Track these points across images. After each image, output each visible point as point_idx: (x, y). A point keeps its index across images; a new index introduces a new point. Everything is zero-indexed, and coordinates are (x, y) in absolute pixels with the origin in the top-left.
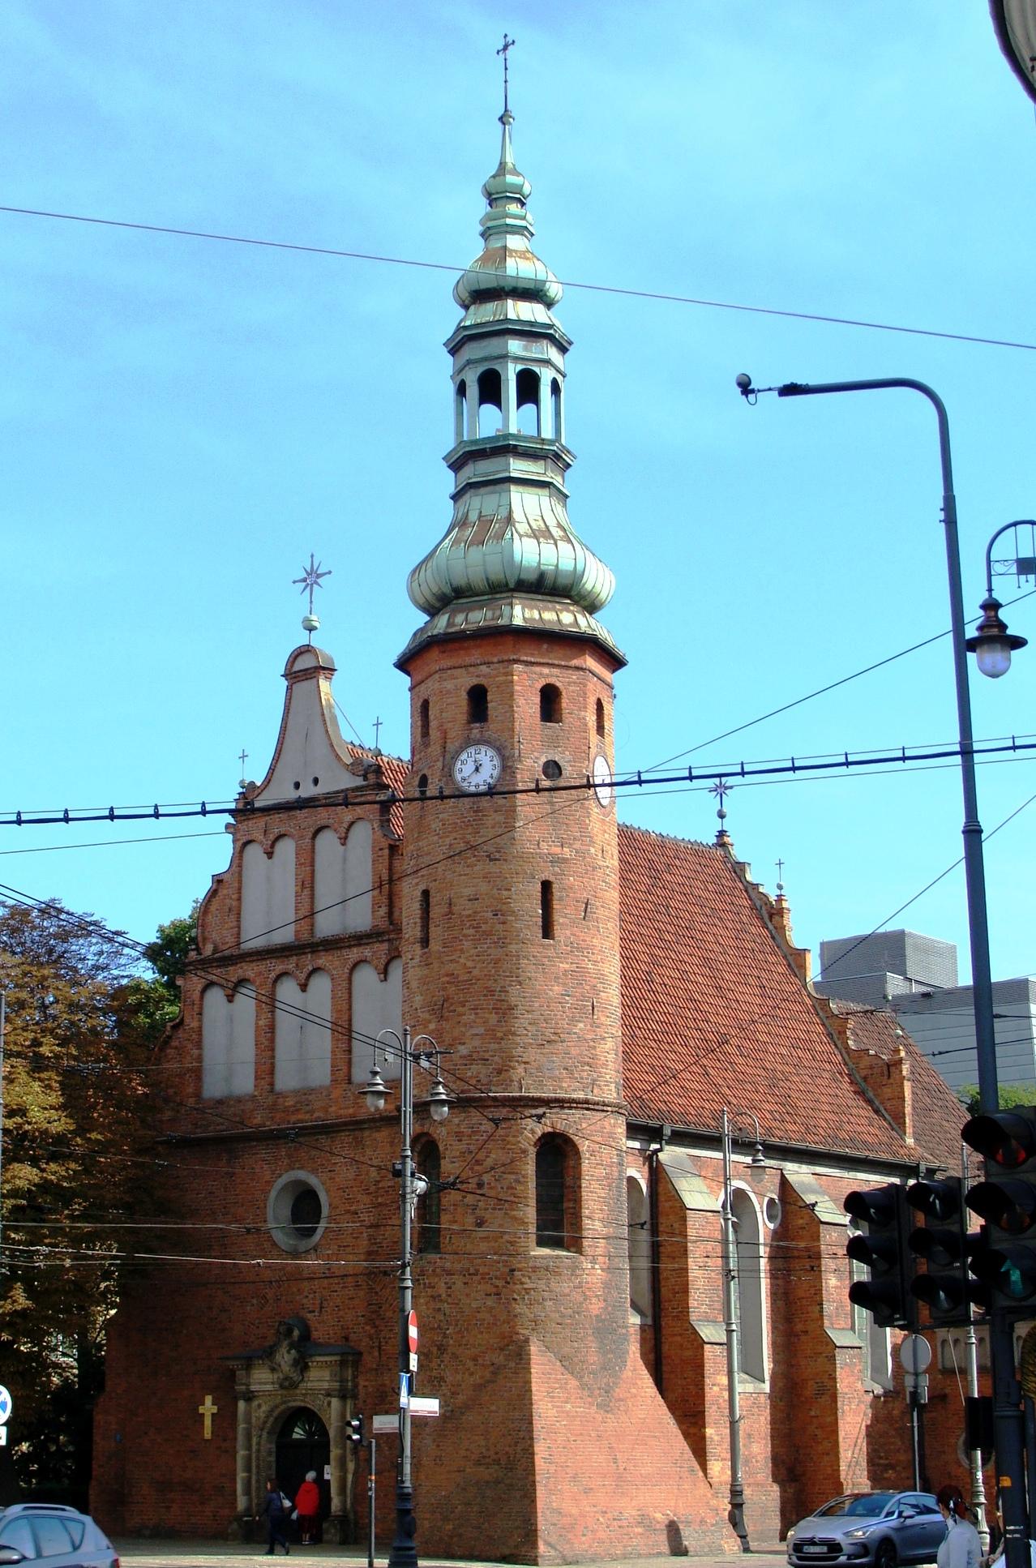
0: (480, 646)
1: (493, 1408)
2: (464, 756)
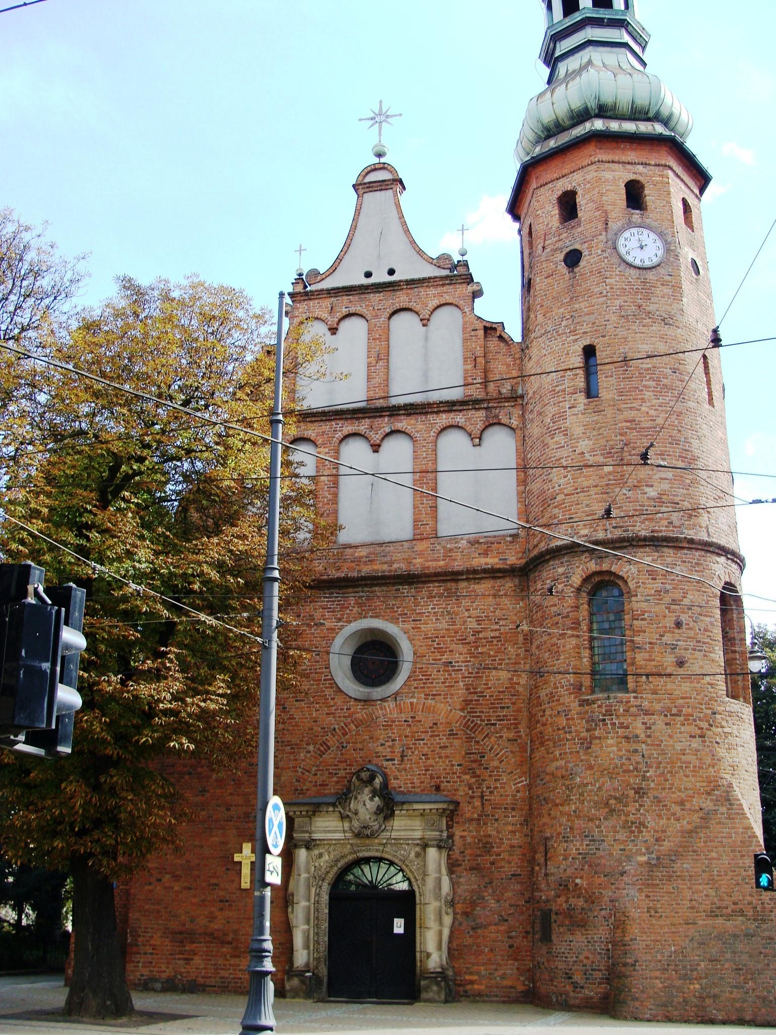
0: (634, 150)
1: (714, 855)
2: (627, 234)
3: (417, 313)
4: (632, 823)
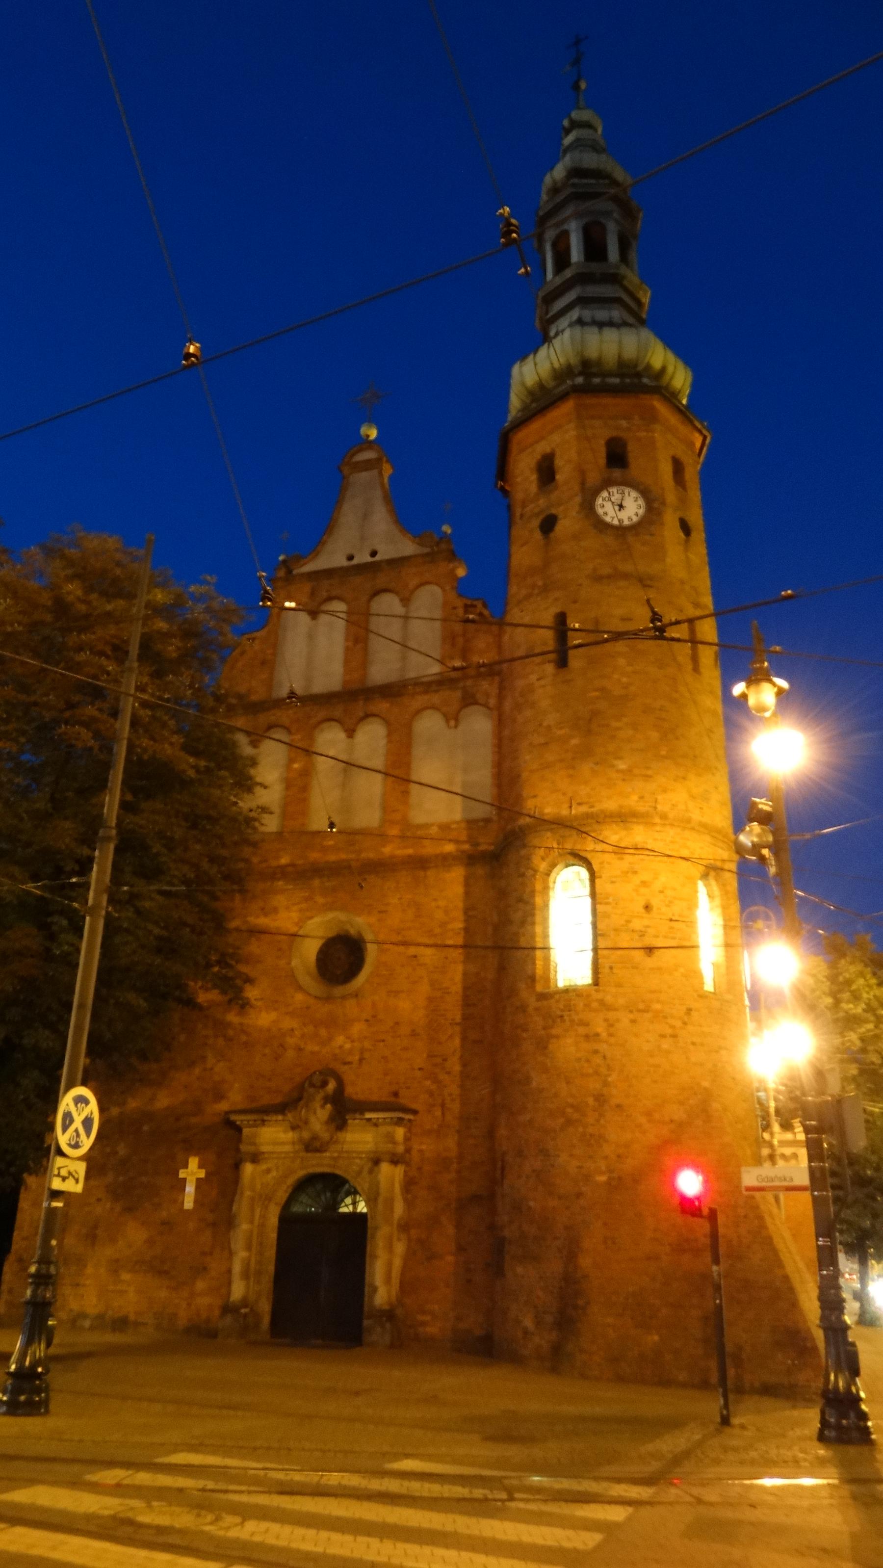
2: (605, 494)
3: (397, 593)
4: (591, 1135)
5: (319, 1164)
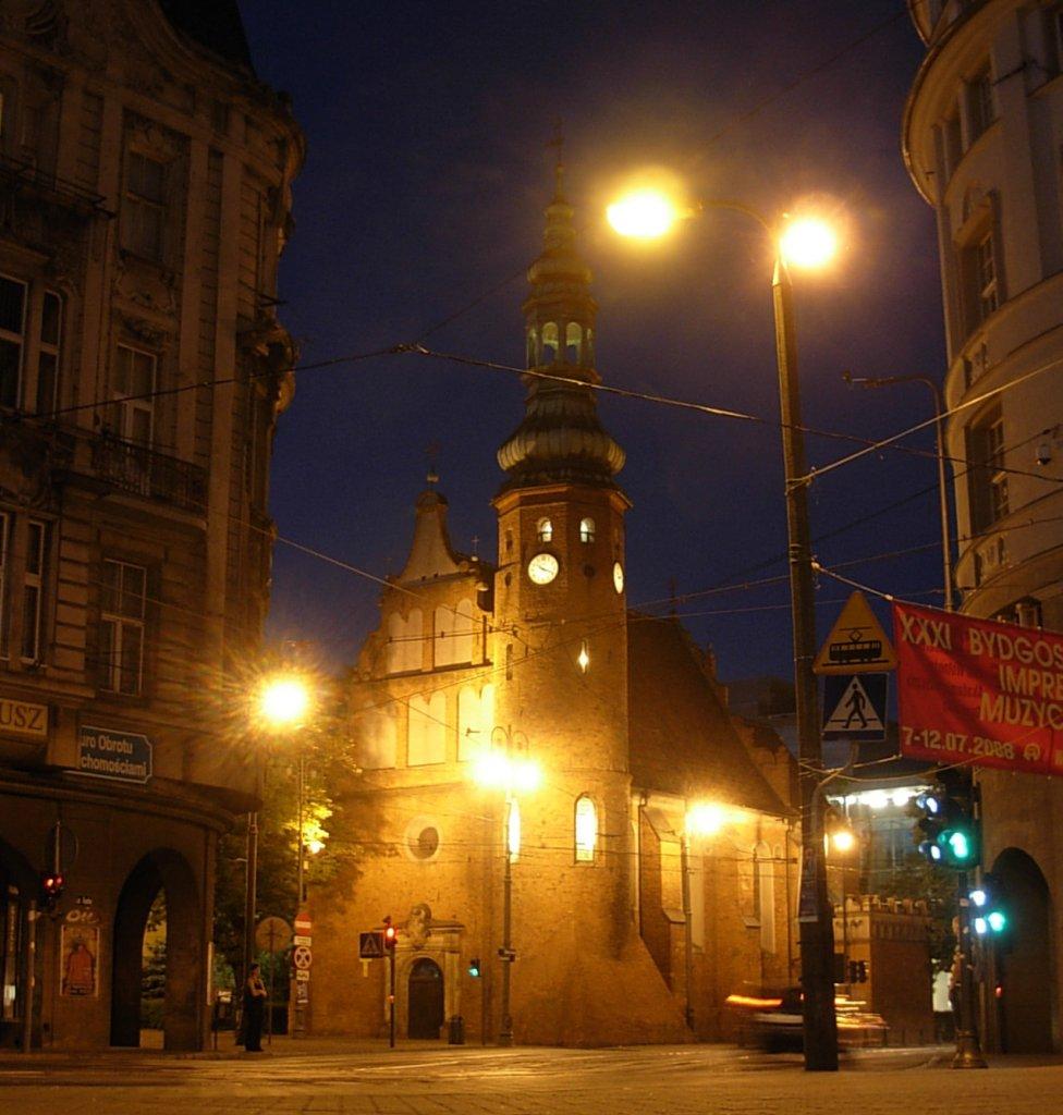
5: (421, 955)
